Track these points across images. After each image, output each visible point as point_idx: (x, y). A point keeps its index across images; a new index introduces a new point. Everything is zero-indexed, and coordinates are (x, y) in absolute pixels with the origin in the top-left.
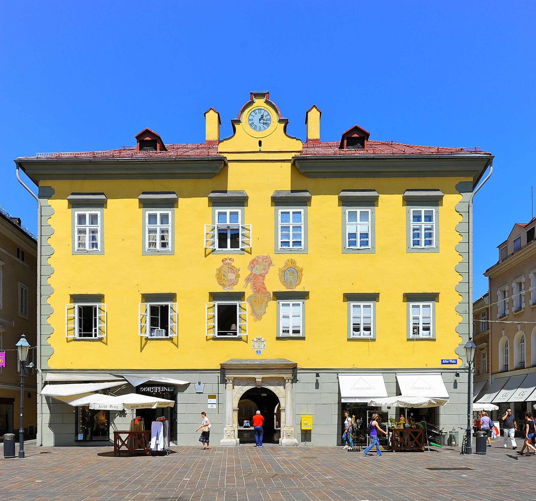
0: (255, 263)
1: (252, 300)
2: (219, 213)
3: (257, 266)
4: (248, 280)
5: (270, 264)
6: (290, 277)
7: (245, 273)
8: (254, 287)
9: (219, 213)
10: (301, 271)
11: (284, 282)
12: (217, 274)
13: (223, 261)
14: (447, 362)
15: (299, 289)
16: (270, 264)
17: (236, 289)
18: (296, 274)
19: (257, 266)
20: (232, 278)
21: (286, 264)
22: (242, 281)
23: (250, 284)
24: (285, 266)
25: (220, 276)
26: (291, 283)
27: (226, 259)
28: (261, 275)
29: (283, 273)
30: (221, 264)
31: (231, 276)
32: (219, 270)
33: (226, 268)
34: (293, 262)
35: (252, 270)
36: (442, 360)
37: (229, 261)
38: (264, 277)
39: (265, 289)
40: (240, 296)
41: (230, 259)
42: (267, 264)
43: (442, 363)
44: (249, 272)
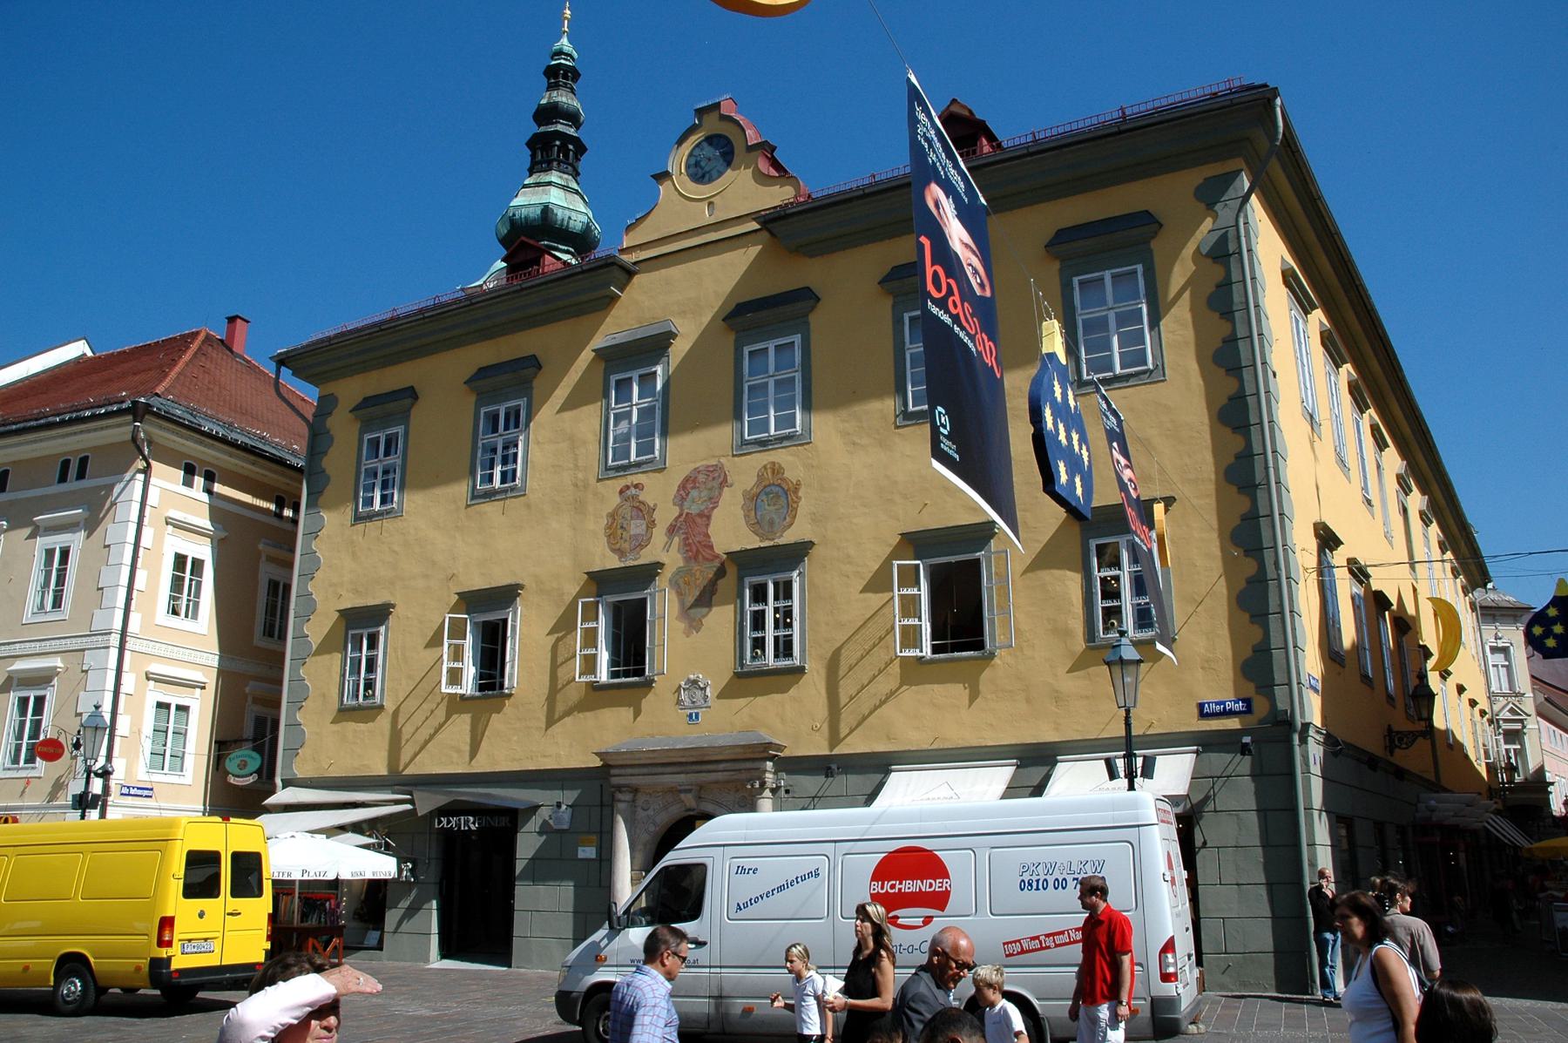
0: (689, 486)
1: (681, 582)
2: (618, 382)
3: (694, 493)
4: (672, 530)
5: (724, 483)
6: (768, 510)
7: (666, 514)
8: (686, 544)
9: (618, 382)
10: (796, 490)
11: (757, 525)
12: (609, 527)
13: (621, 492)
14: (1219, 708)
15: (788, 537)
16: (724, 483)
17: (645, 557)
18: (783, 501)
19: (694, 493)
20: (638, 531)
21: (760, 477)
22: (659, 535)
23: (676, 539)
24: (757, 484)
25: (615, 531)
26: (771, 523)
27: (628, 487)
28: (701, 515)
29: (753, 500)
30: (617, 500)
31: (637, 527)
32: (612, 516)
33: (627, 510)
34: (776, 469)
35: (681, 506)
36: (1201, 706)
37: (633, 491)
38: (709, 517)
39: (711, 547)
40: (648, 573)
41: (636, 486)
42: (716, 484)
43: (1203, 715)
44: (676, 511)
